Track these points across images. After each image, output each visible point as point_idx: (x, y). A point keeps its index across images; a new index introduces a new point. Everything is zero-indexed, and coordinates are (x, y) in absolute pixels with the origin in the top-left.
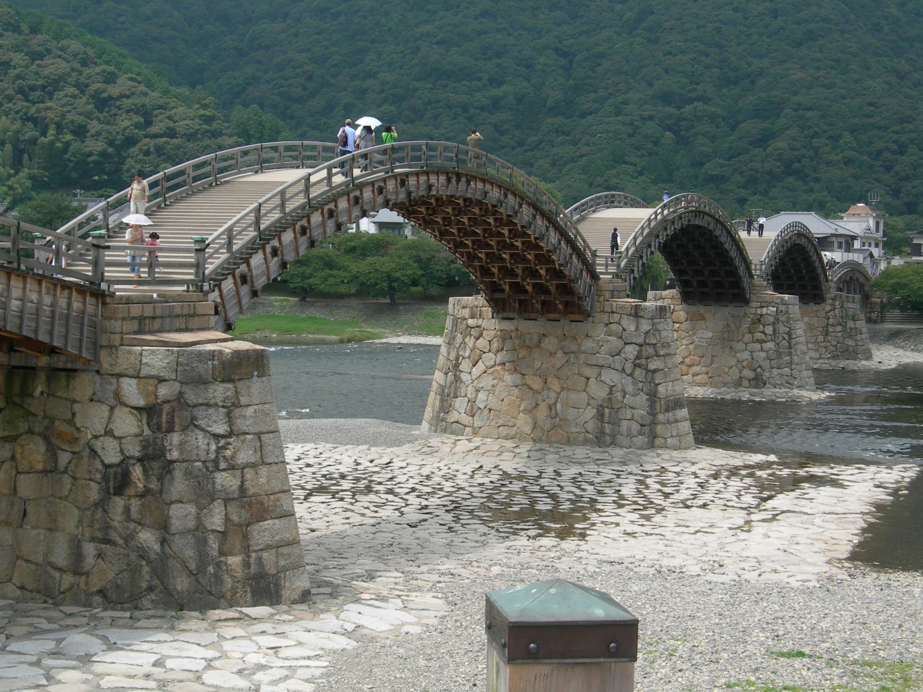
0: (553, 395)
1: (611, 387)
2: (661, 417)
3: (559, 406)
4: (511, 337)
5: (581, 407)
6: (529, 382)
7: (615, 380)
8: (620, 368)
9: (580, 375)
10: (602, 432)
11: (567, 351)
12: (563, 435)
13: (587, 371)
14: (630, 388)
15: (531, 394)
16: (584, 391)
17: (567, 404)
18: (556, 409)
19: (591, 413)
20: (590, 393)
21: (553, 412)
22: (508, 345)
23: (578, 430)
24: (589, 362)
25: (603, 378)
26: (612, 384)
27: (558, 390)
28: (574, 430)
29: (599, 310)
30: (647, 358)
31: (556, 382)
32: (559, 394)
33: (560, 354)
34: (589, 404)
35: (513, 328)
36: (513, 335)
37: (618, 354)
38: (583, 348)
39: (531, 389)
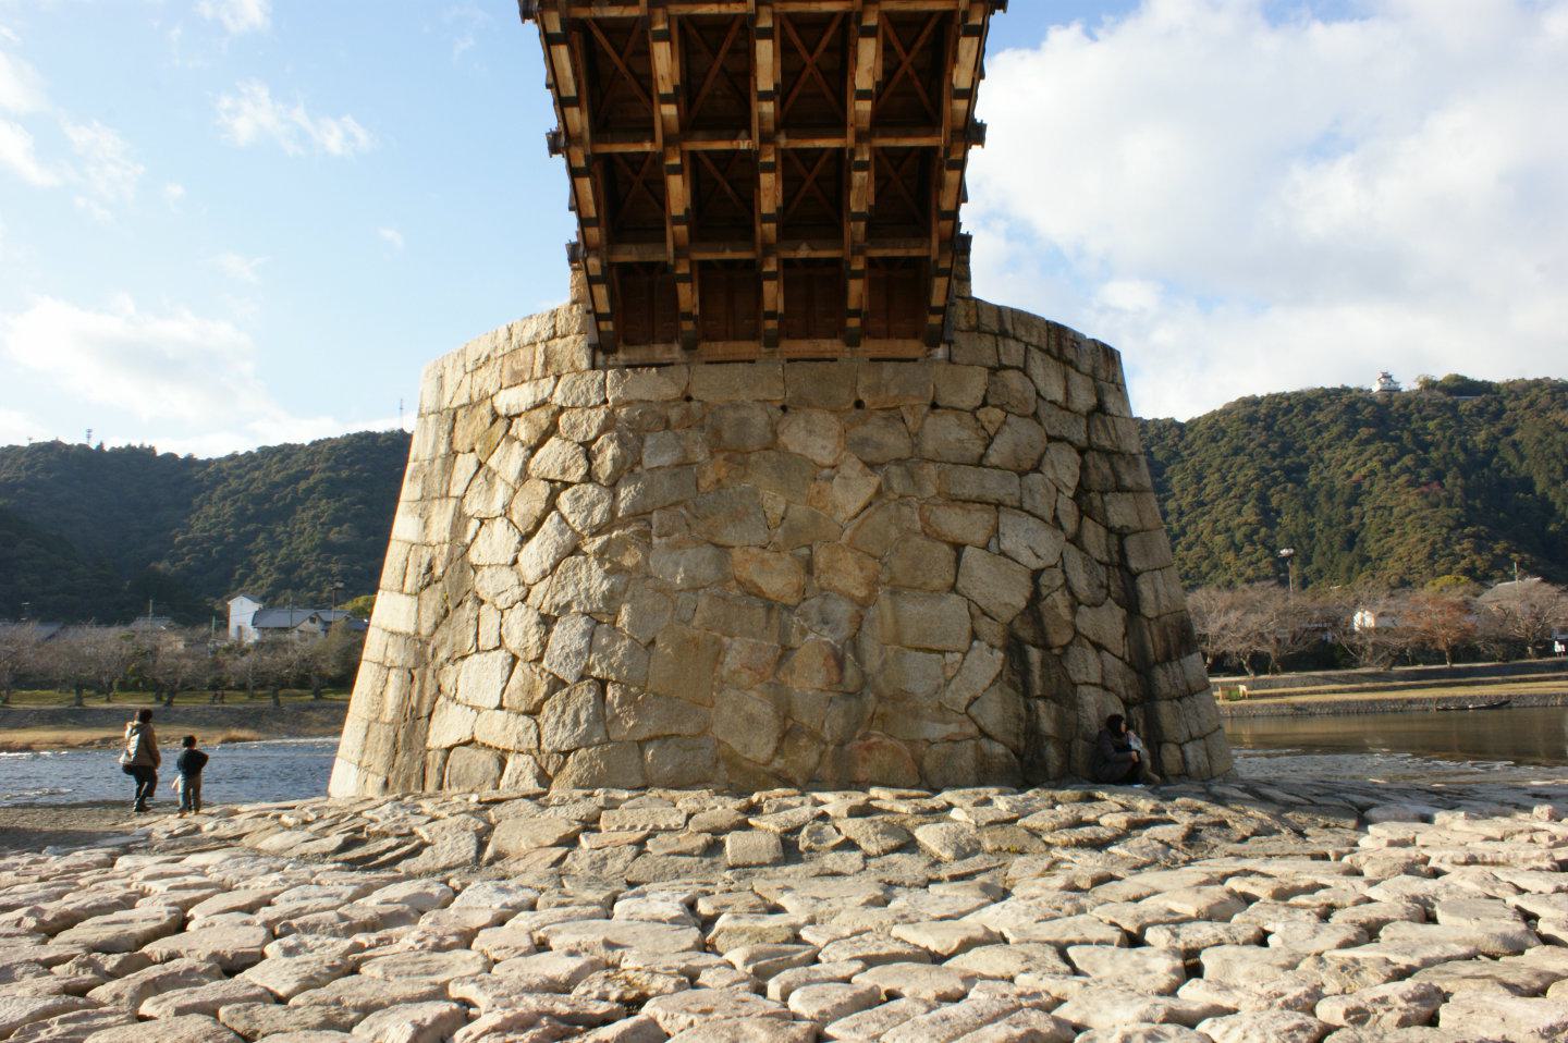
0: (842, 610)
1: (1036, 575)
2: (1162, 678)
3: (870, 646)
4: (667, 425)
5: (949, 644)
6: (751, 572)
7: (1041, 552)
8: (1048, 515)
9: (932, 534)
10: (1032, 732)
11: (873, 455)
12: (897, 753)
13: (955, 522)
14: (1080, 581)
15: (761, 612)
16: (953, 589)
17: (897, 639)
18: (859, 660)
19: (986, 664)
20: (975, 595)
21: (850, 672)
22: (659, 455)
23: (953, 728)
24: (956, 490)
25: (1007, 544)
26: (1036, 564)
27: (861, 593)
28: (936, 731)
29: (963, 325)
30: (1103, 493)
31: (848, 562)
32: (864, 604)
33: (852, 468)
34: (974, 636)
35: (671, 391)
36: (674, 414)
37: (1037, 469)
38: (929, 446)
39: (753, 592)
